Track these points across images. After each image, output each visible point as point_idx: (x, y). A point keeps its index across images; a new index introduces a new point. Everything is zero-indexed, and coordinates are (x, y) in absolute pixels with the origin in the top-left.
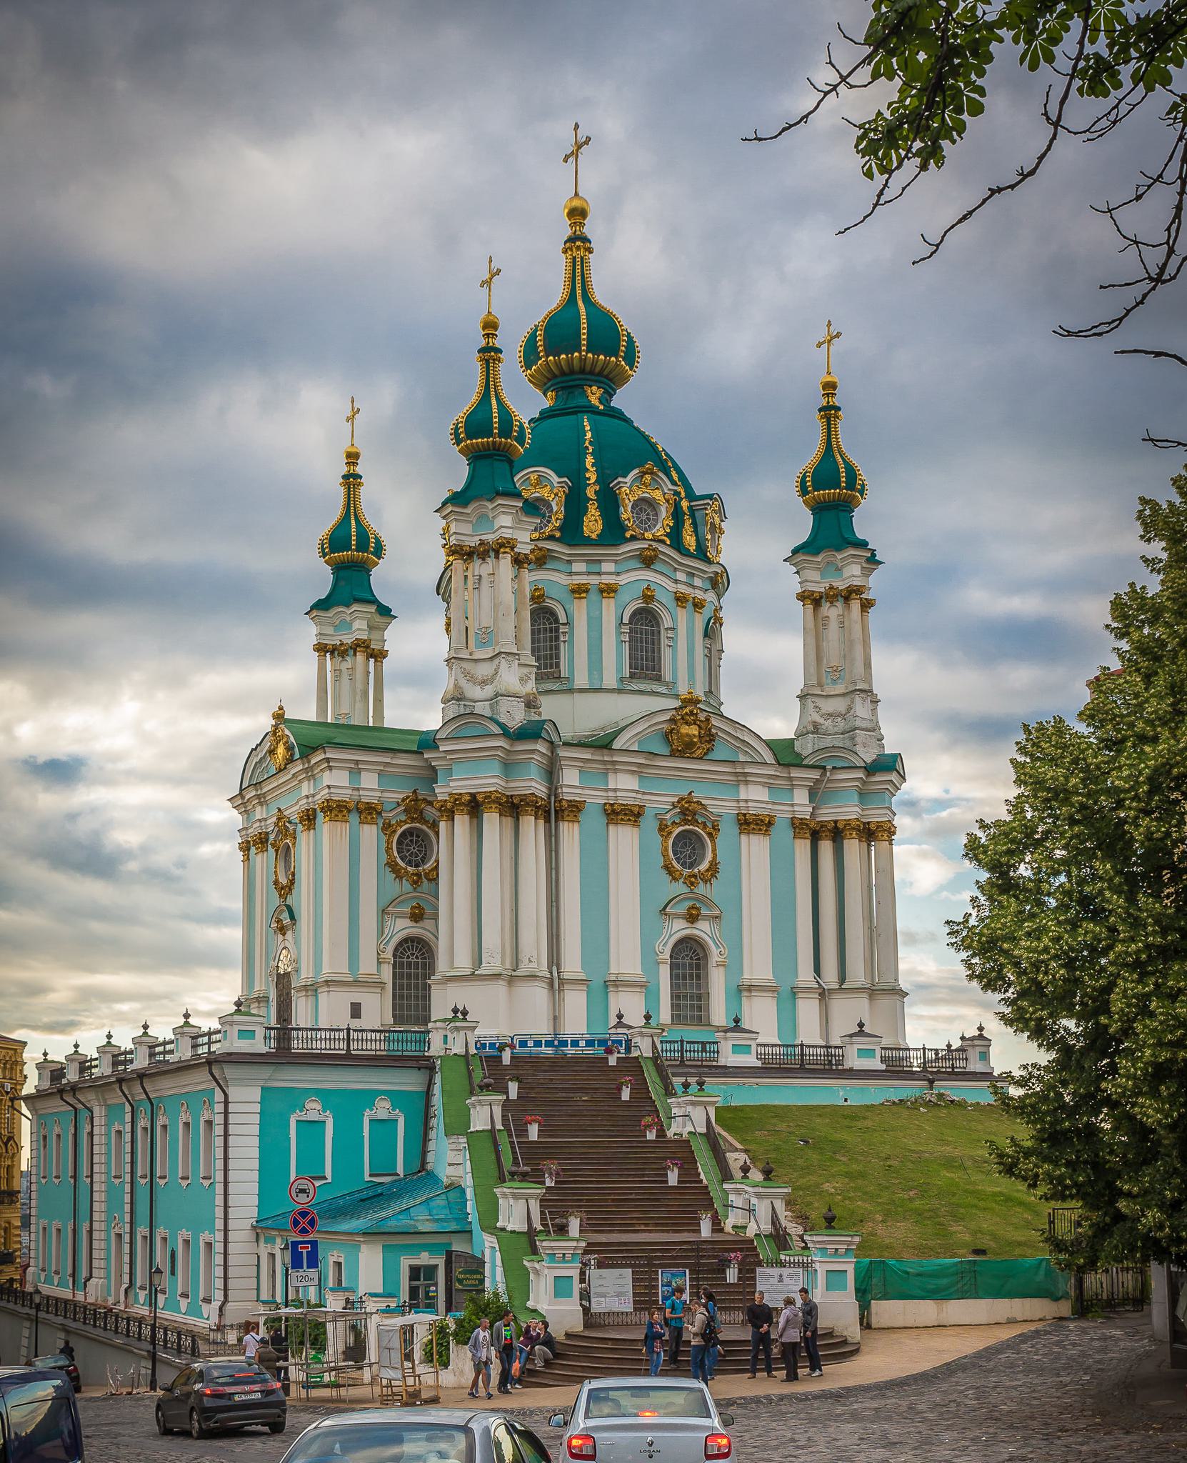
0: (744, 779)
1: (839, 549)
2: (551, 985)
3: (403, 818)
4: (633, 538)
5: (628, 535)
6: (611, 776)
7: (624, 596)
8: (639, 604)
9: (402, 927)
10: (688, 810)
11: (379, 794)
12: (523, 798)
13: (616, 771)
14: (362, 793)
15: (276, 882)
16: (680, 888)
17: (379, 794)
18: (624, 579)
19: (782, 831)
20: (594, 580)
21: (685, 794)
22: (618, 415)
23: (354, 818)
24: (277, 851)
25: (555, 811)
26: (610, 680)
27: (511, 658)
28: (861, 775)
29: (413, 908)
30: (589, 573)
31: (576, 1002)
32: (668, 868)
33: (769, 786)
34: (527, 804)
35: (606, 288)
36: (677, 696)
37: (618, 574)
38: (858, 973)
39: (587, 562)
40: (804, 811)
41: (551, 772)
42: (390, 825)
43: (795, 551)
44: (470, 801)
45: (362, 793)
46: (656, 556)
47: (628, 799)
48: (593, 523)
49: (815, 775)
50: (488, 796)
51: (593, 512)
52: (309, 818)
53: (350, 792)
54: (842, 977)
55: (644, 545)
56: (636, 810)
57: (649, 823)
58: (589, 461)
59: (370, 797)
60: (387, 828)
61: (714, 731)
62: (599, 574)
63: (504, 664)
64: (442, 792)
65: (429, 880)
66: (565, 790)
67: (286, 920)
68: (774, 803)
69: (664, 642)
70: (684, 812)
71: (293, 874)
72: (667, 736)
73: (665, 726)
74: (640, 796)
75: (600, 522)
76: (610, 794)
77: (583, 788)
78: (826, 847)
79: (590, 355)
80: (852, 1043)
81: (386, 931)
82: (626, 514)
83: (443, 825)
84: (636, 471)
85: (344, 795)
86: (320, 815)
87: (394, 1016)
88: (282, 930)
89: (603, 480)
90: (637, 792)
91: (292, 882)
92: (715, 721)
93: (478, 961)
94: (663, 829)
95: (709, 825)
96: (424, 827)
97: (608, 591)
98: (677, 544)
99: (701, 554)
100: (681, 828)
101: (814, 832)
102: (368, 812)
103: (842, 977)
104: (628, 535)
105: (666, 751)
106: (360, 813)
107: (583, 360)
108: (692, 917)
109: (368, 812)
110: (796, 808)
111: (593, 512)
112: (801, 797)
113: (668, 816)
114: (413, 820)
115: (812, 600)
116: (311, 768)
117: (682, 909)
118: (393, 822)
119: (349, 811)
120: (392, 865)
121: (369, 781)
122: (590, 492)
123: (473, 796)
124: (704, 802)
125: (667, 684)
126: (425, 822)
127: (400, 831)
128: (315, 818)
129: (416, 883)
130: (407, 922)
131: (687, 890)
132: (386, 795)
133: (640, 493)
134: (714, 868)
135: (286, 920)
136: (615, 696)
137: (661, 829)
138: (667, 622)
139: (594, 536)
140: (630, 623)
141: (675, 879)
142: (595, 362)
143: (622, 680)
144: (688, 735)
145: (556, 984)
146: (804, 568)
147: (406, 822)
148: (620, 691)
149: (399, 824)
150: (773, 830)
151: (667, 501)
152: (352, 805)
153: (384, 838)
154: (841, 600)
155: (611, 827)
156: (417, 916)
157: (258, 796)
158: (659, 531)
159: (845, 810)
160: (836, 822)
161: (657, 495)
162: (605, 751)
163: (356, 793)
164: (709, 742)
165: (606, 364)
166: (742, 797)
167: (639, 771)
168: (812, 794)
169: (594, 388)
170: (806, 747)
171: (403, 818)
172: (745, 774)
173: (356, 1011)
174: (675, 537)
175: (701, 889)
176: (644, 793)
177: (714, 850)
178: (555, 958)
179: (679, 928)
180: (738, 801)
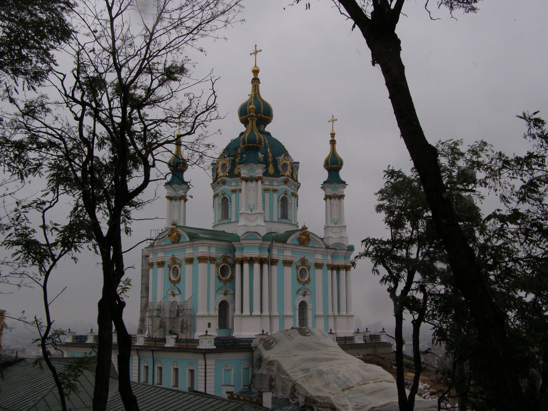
1: (338, 183)
2: (270, 318)
4: (282, 175)
6: (285, 251)
8: (283, 195)
9: (221, 298)
10: (303, 261)
12: (265, 259)
13: (286, 250)
16: (301, 286)
19: (325, 267)
20: (271, 187)
22: (268, 134)
23: (209, 262)
24: (170, 268)
25: (273, 262)
26: (275, 219)
28: (346, 252)
30: (270, 185)
31: (276, 322)
32: (298, 280)
33: (322, 254)
35: (265, 95)
36: (292, 224)
37: (278, 186)
38: (343, 313)
39: (270, 182)
40: (330, 262)
41: (270, 250)
43: (325, 182)
47: (289, 259)
48: (271, 170)
49: (333, 251)
50: (256, 258)
51: (271, 166)
52: (190, 261)
54: (339, 311)
55: (285, 178)
57: (294, 266)
59: (213, 256)
60: (218, 265)
62: (273, 185)
63: (260, 216)
67: (177, 292)
69: (289, 207)
71: (180, 277)
72: (299, 239)
73: (298, 236)
82: (280, 167)
83: (238, 266)
84: (283, 155)
85: (206, 255)
86: (196, 261)
87: (219, 326)
89: (274, 157)
91: (179, 280)
92: (311, 235)
93: (251, 310)
94: (297, 268)
97: (275, 191)
98: (292, 178)
99: (296, 181)
102: (212, 260)
103: (339, 311)
105: (297, 243)
107: (261, 117)
108: (304, 295)
109: (212, 260)
111: (271, 166)
112: (329, 258)
114: (224, 262)
115: (327, 197)
116: (193, 245)
117: (301, 292)
119: (207, 259)
120: (219, 277)
122: (270, 160)
123: (251, 258)
125: (290, 220)
128: (193, 260)
129: (225, 283)
130: (222, 296)
133: (284, 162)
134: (309, 280)
137: (297, 268)
138: (290, 202)
141: (300, 283)
143: (278, 219)
145: (271, 317)
148: (278, 222)
149: (221, 264)
155: (285, 268)
156: (225, 294)
158: (288, 173)
159: (340, 262)
161: (288, 162)
165: (267, 118)
168: (332, 256)
170: (330, 243)
174: (292, 175)
175: (306, 286)
178: (270, 309)
179: (301, 298)
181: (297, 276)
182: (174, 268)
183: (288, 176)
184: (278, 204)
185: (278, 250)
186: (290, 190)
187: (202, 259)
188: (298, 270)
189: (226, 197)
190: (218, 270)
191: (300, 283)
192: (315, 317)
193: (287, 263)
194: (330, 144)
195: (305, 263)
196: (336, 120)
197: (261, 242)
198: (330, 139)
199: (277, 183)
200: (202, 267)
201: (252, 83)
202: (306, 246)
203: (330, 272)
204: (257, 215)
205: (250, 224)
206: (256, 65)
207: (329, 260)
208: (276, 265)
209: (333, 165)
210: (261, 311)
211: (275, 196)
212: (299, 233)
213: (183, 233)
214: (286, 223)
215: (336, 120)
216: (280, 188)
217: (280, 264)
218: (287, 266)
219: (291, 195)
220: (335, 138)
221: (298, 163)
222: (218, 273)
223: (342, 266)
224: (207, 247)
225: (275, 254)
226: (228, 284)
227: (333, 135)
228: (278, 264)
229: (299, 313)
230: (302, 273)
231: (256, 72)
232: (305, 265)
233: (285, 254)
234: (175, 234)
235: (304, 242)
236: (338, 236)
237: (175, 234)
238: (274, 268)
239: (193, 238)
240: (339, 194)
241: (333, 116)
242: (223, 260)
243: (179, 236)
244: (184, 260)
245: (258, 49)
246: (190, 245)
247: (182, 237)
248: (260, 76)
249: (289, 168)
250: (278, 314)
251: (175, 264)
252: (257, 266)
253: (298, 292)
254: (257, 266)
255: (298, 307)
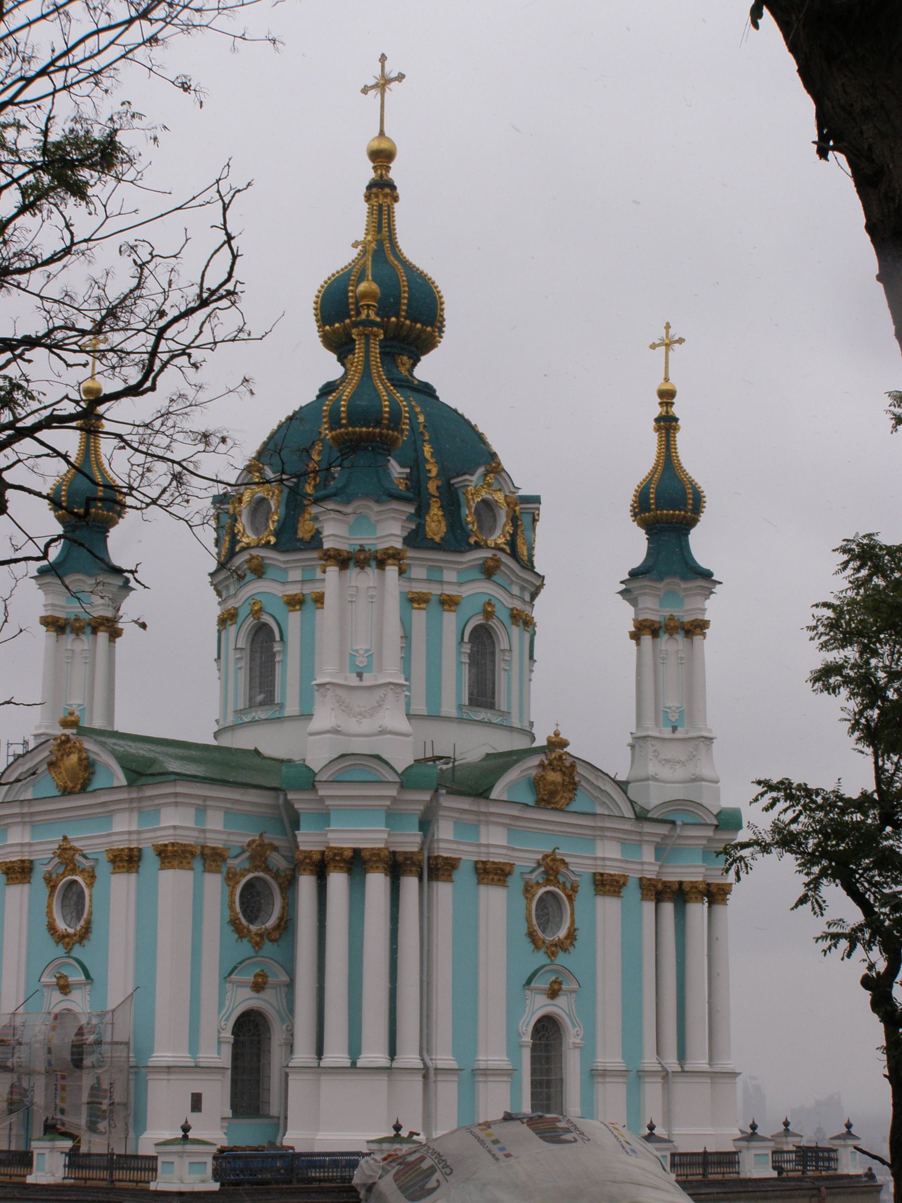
0: (600, 833)
1: (684, 578)
2: (425, 1077)
3: (247, 865)
4: (477, 546)
5: (472, 540)
6: (483, 829)
7: (466, 609)
9: (243, 999)
10: (552, 867)
11: (225, 837)
12: (409, 857)
13: (487, 823)
14: (208, 835)
15: (52, 928)
16: (541, 958)
17: (225, 837)
18: (465, 591)
19: (632, 891)
20: (435, 590)
21: (549, 850)
22: (427, 391)
23: (198, 864)
24: (53, 888)
25: (438, 869)
26: (449, 708)
27: (399, 690)
28: (710, 833)
29: (257, 976)
30: (429, 581)
31: (447, 1092)
32: (531, 935)
33: (622, 842)
34: (413, 864)
35: (418, 242)
36: (511, 729)
37: (460, 584)
39: (430, 568)
40: (651, 872)
41: (426, 824)
42: (235, 874)
44: (353, 857)
45: (208, 835)
46: (498, 567)
48: (436, 525)
49: (663, 830)
50: (375, 853)
51: (435, 511)
52: (127, 860)
53: (196, 834)
54: (682, 1055)
55: (488, 554)
56: (507, 869)
57: (515, 882)
58: (427, 450)
59: (214, 841)
60: (231, 878)
61: (577, 779)
62: (441, 582)
63: (391, 696)
64: (309, 840)
65: (272, 941)
66: (442, 845)
67: (76, 976)
68: (627, 862)
69: (500, 665)
70: (546, 872)
71: (89, 923)
72: (536, 784)
73: (534, 772)
74: (510, 853)
75: (443, 524)
76: (483, 850)
77: (458, 843)
78: (668, 908)
79: (408, 322)
80: (748, 1148)
81: (227, 1003)
82: (468, 515)
83: (306, 884)
84: (481, 470)
85: (189, 838)
86: (150, 860)
87: (234, 1106)
88: (64, 988)
89: (447, 475)
90: (508, 848)
91: (86, 931)
92: (580, 769)
93: (355, 1049)
94: (528, 890)
95: (568, 885)
96: (267, 877)
98: (514, 554)
99: (529, 566)
100: (544, 890)
101: (659, 892)
102: (212, 858)
103: (682, 1055)
104: (472, 540)
105: (531, 801)
106: (205, 860)
107: (399, 326)
108: (553, 993)
109: (212, 858)
110: (646, 867)
111: (435, 511)
112: (648, 855)
113: (533, 877)
114: (256, 868)
115: (643, 629)
116: (140, 799)
118: (238, 870)
119: (193, 855)
120: (234, 923)
121: (215, 822)
122: (432, 487)
123: (357, 852)
124: (567, 860)
126: (267, 870)
127: (244, 881)
128: (140, 858)
129: (257, 945)
130: (247, 992)
131: (548, 961)
132: (232, 838)
133: (484, 494)
134: (571, 936)
135: (76, 976)
136: (454, 727)
138: (503, 644)
139: (437, 539)
140: (469, 642)
141: (537, 948)
142: (411, 328)
143: (460, 707)
144: (553, 783)
145: (426, 1073)
146: (645, 594)
147: (249, 871)
148: (460, 720)
150: (624, 892)
151: (508, 505)
152: (198, 851)
153: (227, 890)
154: (682, 633)
155: (483, 889)
156: (258, 987)
157: (23, 815)
158: (498, 537)
159: (690, 870)
160: (681, 883)
161: (499, 497)
162: (482, 801)
163: (202, 835)
164: (570, 791)
165: (422, 331)
166: (599, 855)
167: (511, 826)
168: (660, 850)
169: (405, 358)
170: (653, 798)
171: (247, 865)
172: (602, 829)
173: (196, 1103)
174: (512, 544)
175: (562, 959)
176: (514, 849)
177: (572, 914)
179: (539, 1006)
180: (595, 859)
181: (528, 920)
182: (69, 885)
183: (498, 548)
184: (460, 653)
185: (457, 823)
186: (505, 601)
187: (175, 855)
188: (529, 900)
189: (265, 625)
190: (232, 894)
191: (537, 948)
192: (594, 1075)
193: (492, 873)
194: (658, 429)
195: (557, 872)
196: (681, 341)
197: (393, 792)
198: (657, 411)
199: (456, 575)
200: (174, 884)
201: (368, 198)
202: (562, 810)
203: (649, 907)
204: (380, 693)
205: (352, 725)
206: (382, 133)
207: (646, 863)
208: (449, 879)
209: (668, 509)
210: (392, 1052)
211: (450, 621)
212: (535, 761)
213: (105, 758)
214: (489, 724)
215: (681, 341)
216: (465, 591)
217: (464, 875)
218: (492, 882)
219: (507, 621)
220: (676, 410)
221: (536, 500)
222: (231, 907)
223: (694, 885)
224: (192, 811)
225: (447, 838)
226: (269, 948)
227: (667, 396)
228: (456, 875)
229: (534, 1060)
230: (547, 910)
231: (382, 157)
232: (557, 883)
233: (483, 841)
234: (74, 758)
235: (553, 794)
236: (680, 773)
237: (74, 758)
238: (443, 891)
239: (141, 774)
240: (687, 619)
241: (668, 327)
242: (252, 858)
243: (88, 766)
244: (104, 859)
245: (392, 70)
246: (131, 800)
247: (99, 769)
248: (396, 173)
249: (503, 517)
250: (454, 1065)
251: (73, 871)
252: (377, 883)
253: (529, 982)
254: (377, 883)
255: (527, 1039)
